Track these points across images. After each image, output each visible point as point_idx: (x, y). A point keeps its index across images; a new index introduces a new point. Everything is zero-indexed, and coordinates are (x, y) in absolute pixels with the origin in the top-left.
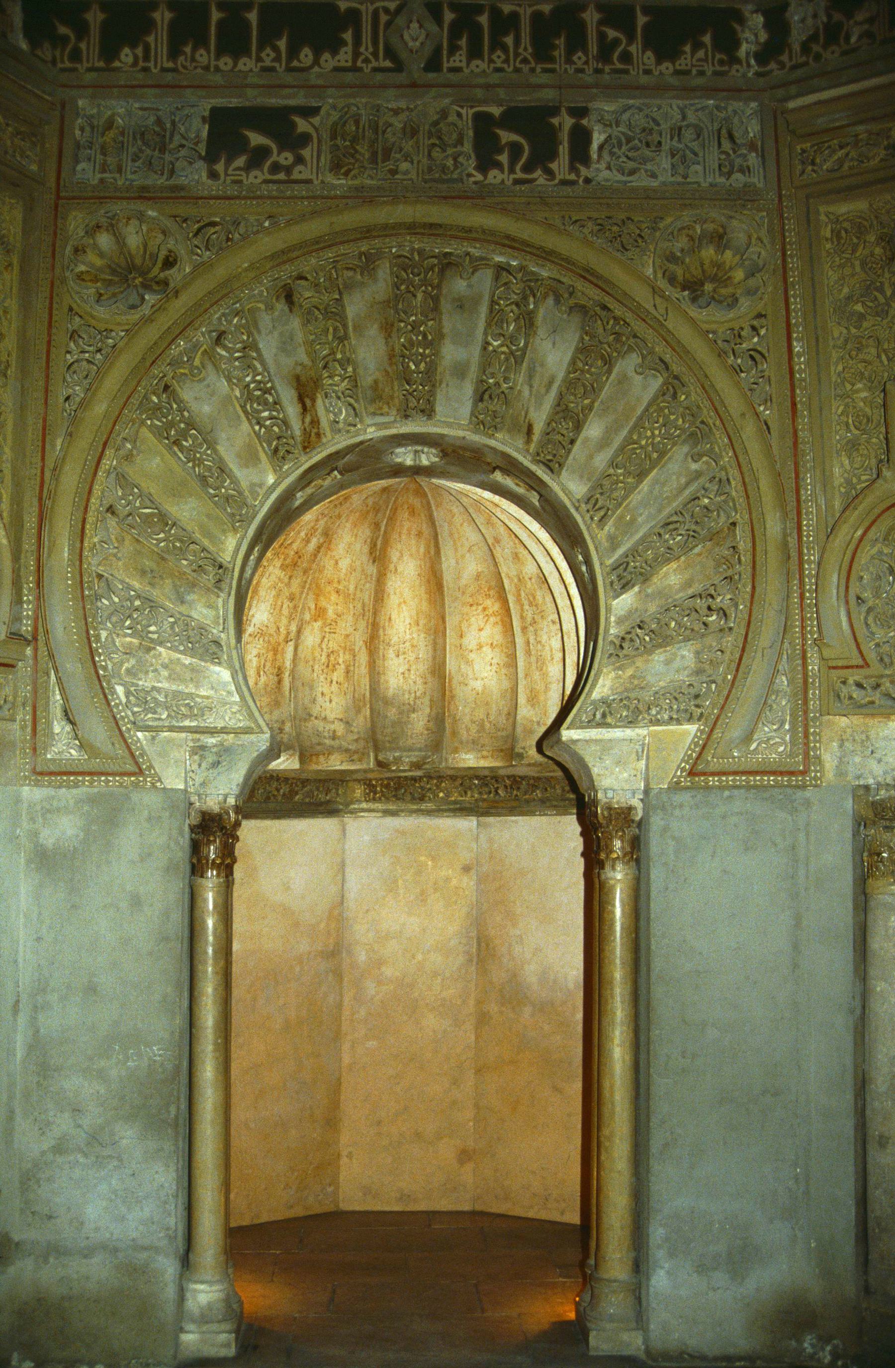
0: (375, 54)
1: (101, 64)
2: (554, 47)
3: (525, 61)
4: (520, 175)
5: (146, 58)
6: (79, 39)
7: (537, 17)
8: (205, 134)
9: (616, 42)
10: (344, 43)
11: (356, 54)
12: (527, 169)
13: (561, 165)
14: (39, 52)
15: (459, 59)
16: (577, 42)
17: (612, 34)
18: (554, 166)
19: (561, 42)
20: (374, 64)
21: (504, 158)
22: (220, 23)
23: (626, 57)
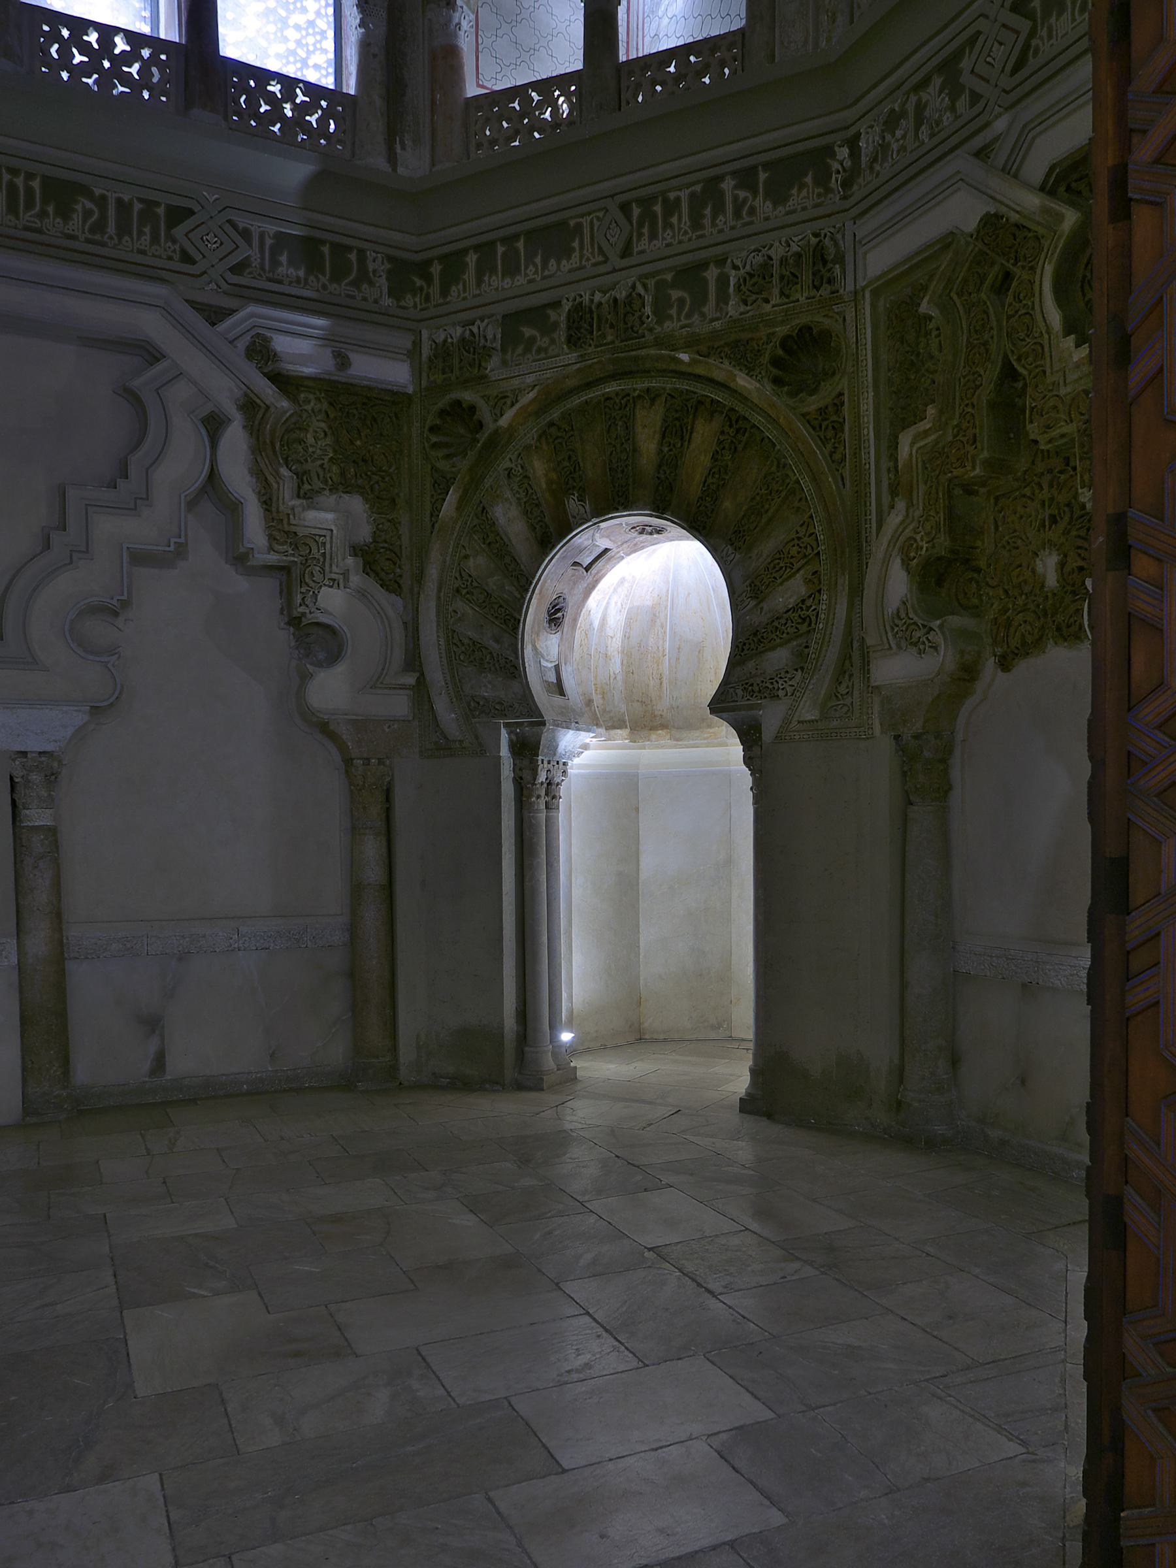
0: (593, 253)
1: (441, 301)
2: (704, 216)
3: (686, 233)
4: (684, 322)
5: (465, 291)
6: (429, 286)
7: (693, 195)
8: (499, 336)
9: (745, 200)
10: (573, 249)
11: (581, 257)
12: (688, 316)
13: (709, 308)
14: (403, 303)
15: (644, 244)
16: (719, 209)
17: (742, 194)
18: (705, 310)
19: (708, 211)
20: (593, 261)
21: (673, 312)
22: (504, 254)
23: (752, 211)
